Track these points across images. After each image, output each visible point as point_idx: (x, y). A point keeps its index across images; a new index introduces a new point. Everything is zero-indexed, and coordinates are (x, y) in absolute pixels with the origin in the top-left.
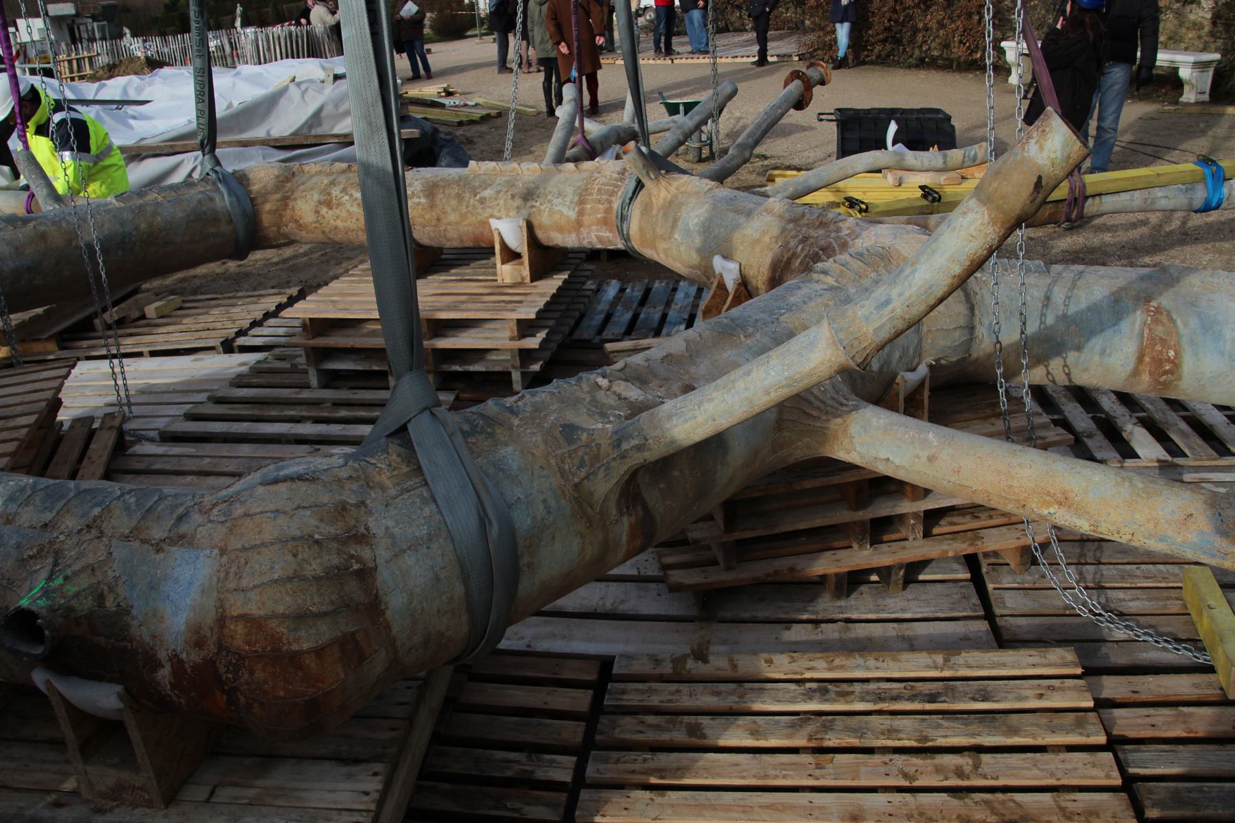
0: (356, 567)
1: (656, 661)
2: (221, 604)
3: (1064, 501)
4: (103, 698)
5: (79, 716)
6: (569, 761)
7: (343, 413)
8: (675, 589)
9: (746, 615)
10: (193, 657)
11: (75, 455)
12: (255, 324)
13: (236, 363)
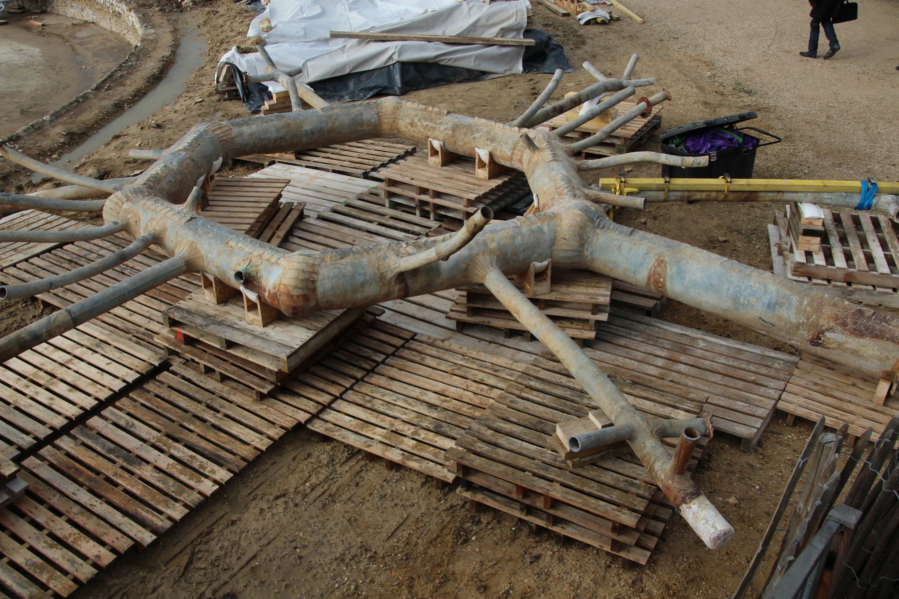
1: (429, 338)
4: (252, 296)
5: (248, 300)
9: (472, 334)
10: (273, 291)
11: (281, 219)
12: (383, 165)
13: (363, 186)
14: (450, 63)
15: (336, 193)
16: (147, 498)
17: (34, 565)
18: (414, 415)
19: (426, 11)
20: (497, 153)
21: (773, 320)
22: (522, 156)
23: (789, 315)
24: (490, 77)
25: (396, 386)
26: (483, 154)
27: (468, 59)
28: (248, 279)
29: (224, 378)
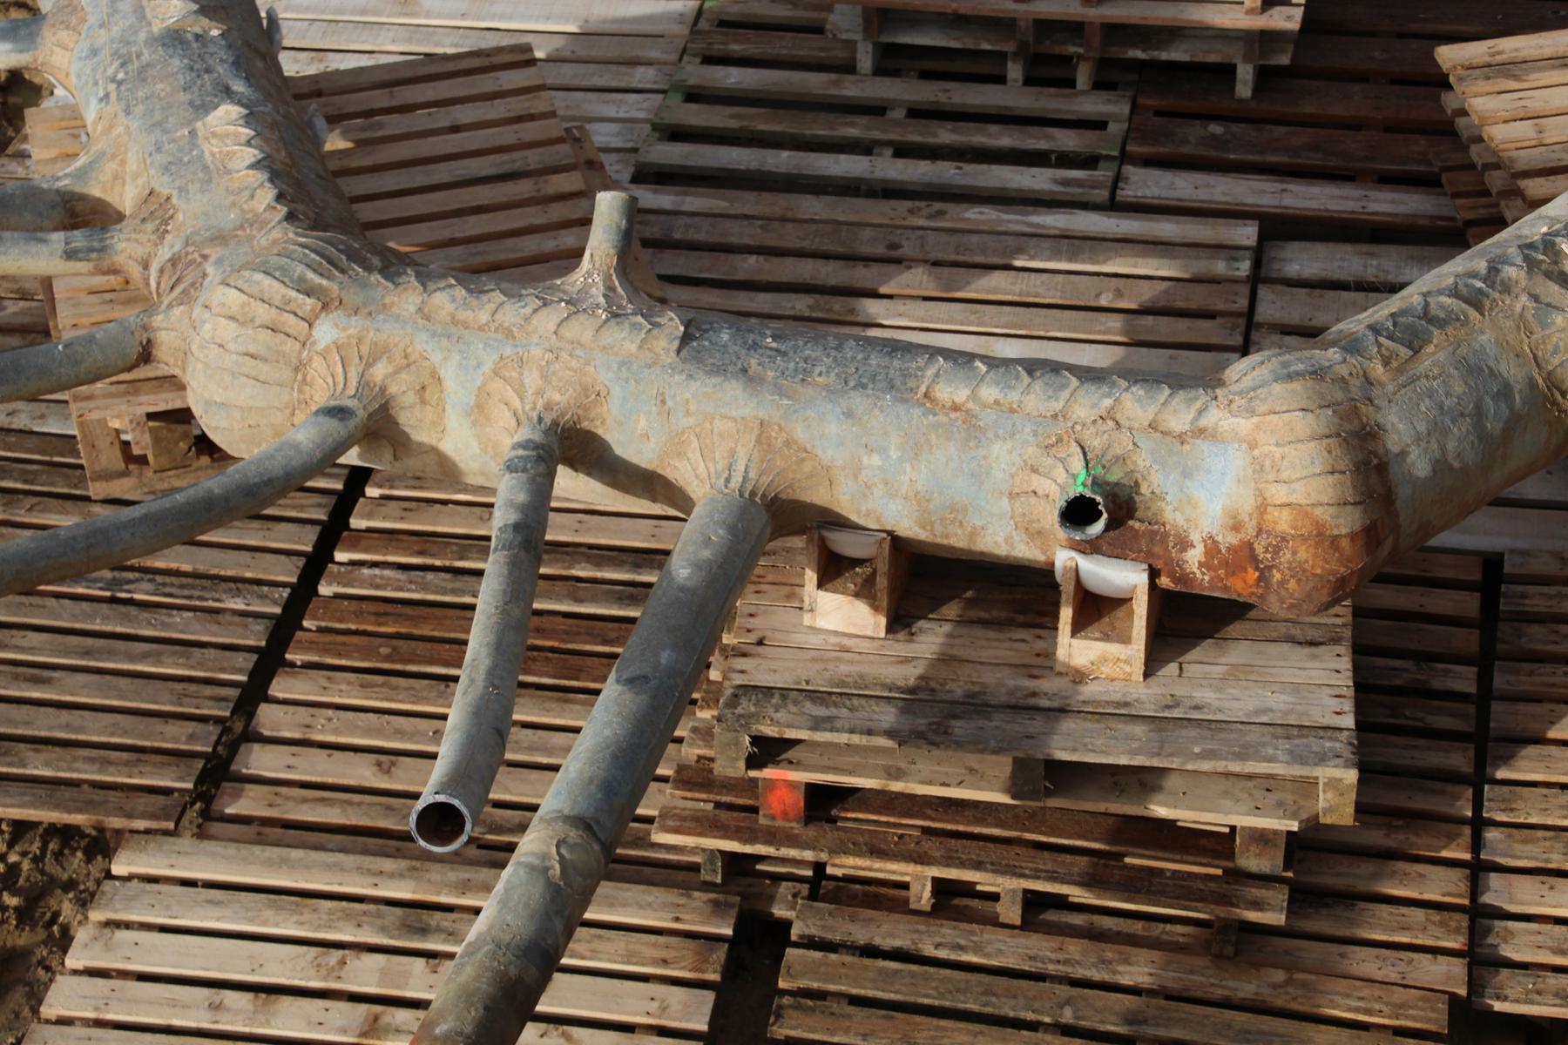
0: (1375, 461)
2: (1260, 494)
6: (1471, 671)
7: (945, 135)
10: (1228, 540)
15: (612, 50)
28: (1106, 511)
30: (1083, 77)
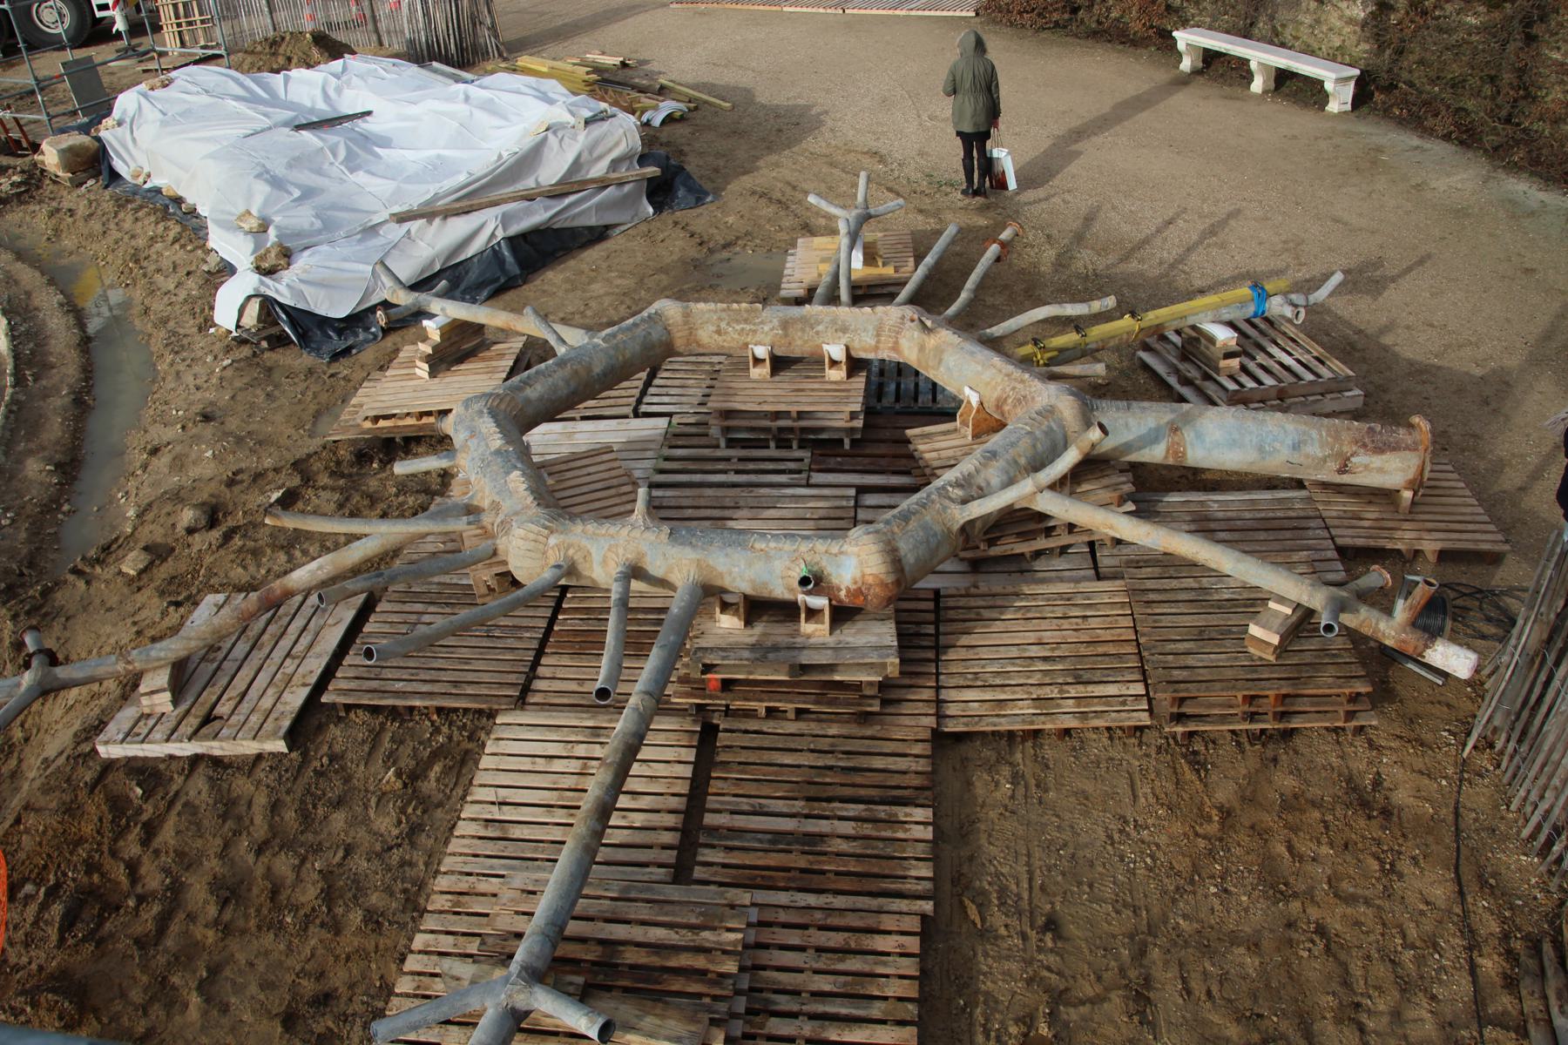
3: (1111, 527)
7: (751, 466)
8: (962, 560)
10: (853, 587)
14: (567, 224)
15: (639, 446)
16: (876, 870)
17: (845, 984)
18: (1039, 675)
19: (500, 157)
20: (856, 345)
21: (1302, 460)
22: (896, 343)
23: (1315, 450)
24: (617, 231)
25: (985, 653)
26: (836, 351)
27: (584, 211)
29: (800, 713)
30: (795, 445)
